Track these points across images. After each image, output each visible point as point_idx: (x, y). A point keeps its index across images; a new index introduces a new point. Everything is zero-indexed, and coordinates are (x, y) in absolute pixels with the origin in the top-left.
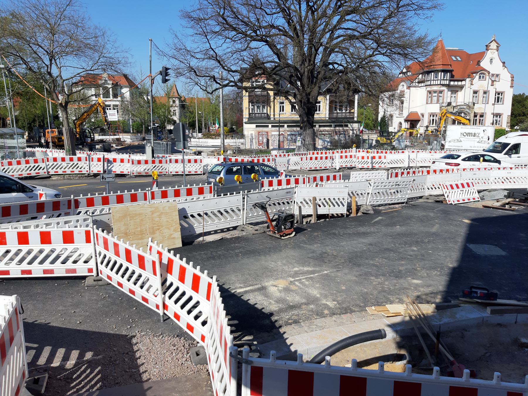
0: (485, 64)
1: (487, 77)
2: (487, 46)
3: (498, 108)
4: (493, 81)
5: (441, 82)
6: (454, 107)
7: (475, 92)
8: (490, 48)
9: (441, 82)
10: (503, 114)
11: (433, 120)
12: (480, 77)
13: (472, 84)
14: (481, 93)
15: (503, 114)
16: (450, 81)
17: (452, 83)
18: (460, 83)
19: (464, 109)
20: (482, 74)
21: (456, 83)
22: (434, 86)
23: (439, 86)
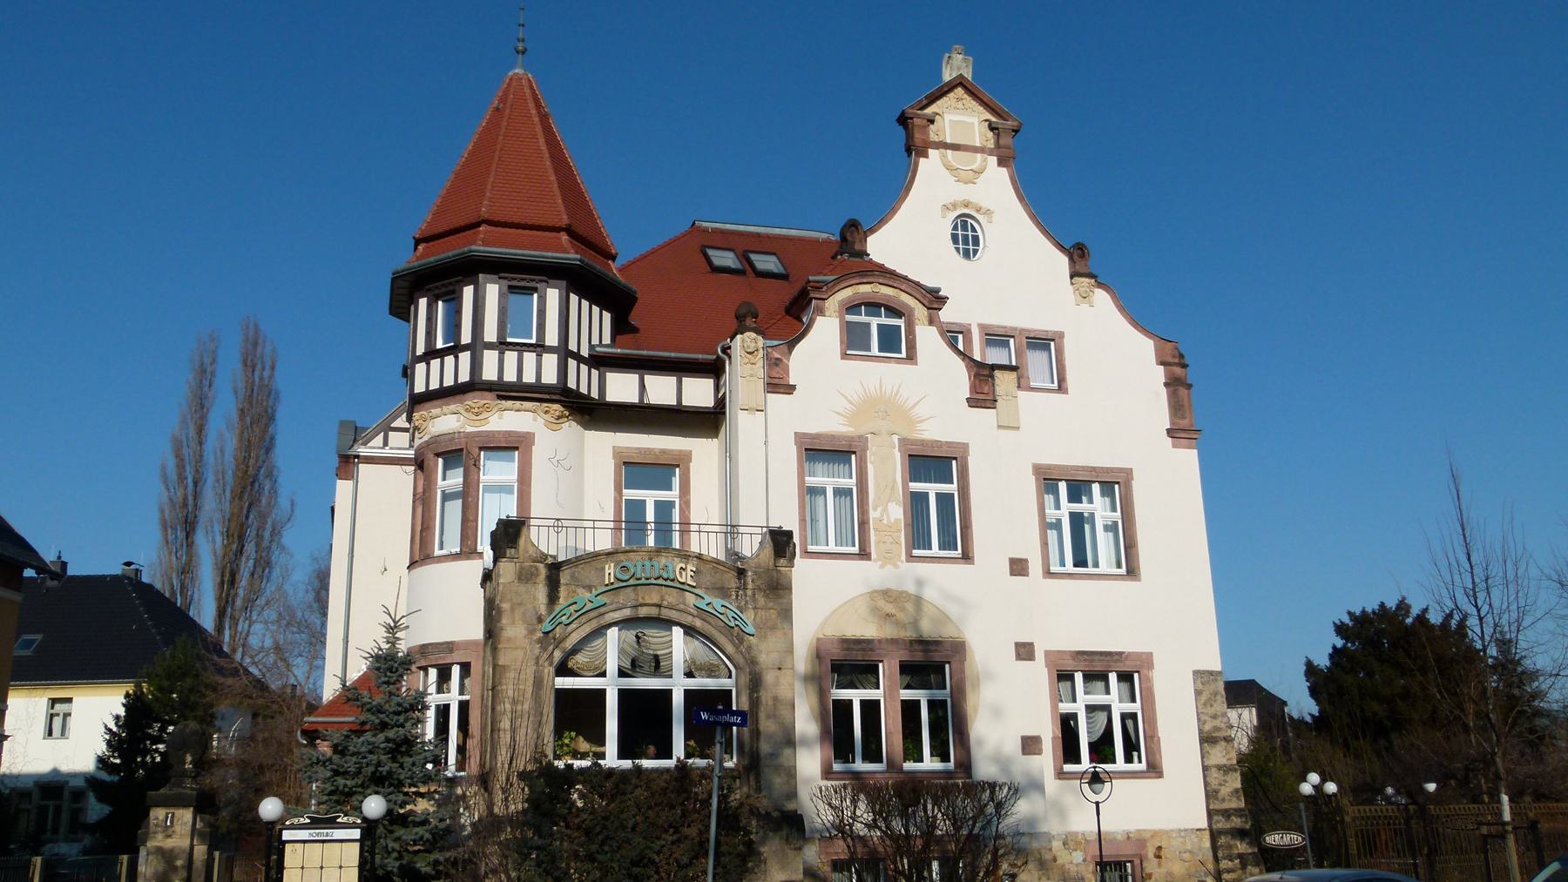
0: (906, 242)
1: (928, 338)
2: (903, 120)
3: (1089, 615)
4: (983, 374)
5: (476, 365)
6: (555, 568)
7: (820, 451)
8: (933, 134)
9: (476, 365)
10: (1146, 660)
11: (443, 711)
12: (854, 339)
13: (778, 385)
14: (886, 473)
15: (1146, 660)
16: (600, 362)
17: (621, 388)
18: (698, 392)
19: (682, 588)
20: (873, 306)
21: (661, 390)
22: (435, 409)
23: (474, 400)
